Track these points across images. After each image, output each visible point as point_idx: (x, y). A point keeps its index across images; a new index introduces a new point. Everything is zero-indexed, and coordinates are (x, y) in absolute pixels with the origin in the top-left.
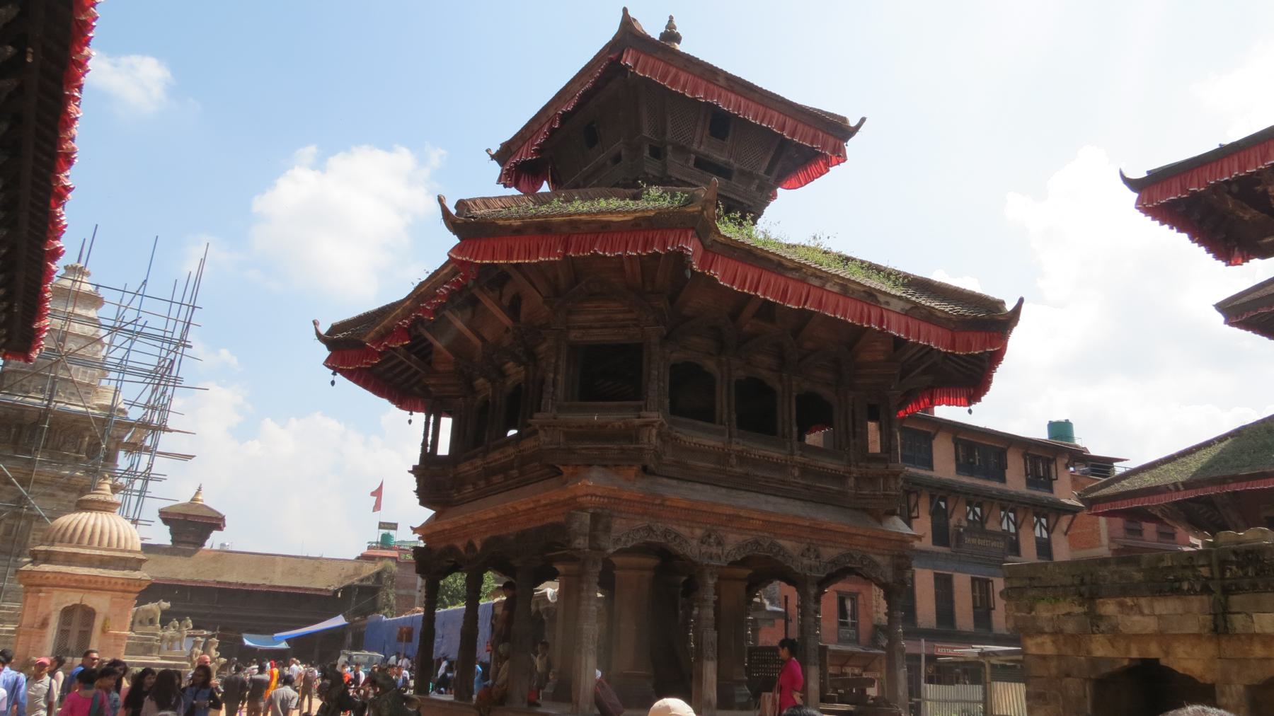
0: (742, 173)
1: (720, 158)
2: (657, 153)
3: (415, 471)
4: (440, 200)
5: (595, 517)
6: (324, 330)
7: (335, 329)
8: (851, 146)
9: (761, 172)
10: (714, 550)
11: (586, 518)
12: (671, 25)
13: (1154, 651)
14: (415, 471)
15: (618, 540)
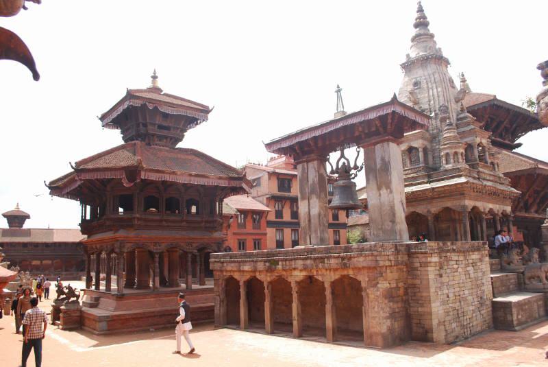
0: (174, 128)
1: (164, 124)
2: (145, 125)
3: (80, 225)
4: (70, 163)
5: (121, 243)
6: (47, 184)
7: (52, 183)
8: (210, 116)
9: (181, 126)
10: (158, 248)
11: (118, 243)
12: (155, 73)
13: (232, 274)
14: (80, 225)
15: (128, 248)
